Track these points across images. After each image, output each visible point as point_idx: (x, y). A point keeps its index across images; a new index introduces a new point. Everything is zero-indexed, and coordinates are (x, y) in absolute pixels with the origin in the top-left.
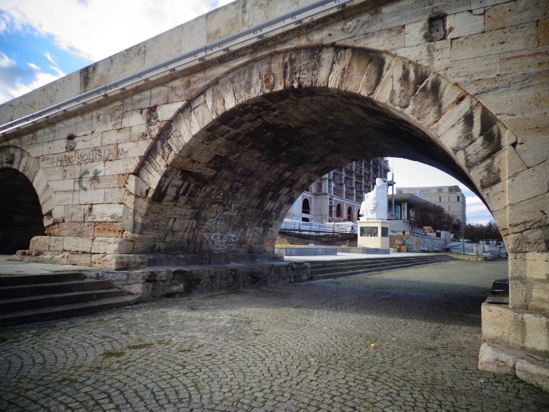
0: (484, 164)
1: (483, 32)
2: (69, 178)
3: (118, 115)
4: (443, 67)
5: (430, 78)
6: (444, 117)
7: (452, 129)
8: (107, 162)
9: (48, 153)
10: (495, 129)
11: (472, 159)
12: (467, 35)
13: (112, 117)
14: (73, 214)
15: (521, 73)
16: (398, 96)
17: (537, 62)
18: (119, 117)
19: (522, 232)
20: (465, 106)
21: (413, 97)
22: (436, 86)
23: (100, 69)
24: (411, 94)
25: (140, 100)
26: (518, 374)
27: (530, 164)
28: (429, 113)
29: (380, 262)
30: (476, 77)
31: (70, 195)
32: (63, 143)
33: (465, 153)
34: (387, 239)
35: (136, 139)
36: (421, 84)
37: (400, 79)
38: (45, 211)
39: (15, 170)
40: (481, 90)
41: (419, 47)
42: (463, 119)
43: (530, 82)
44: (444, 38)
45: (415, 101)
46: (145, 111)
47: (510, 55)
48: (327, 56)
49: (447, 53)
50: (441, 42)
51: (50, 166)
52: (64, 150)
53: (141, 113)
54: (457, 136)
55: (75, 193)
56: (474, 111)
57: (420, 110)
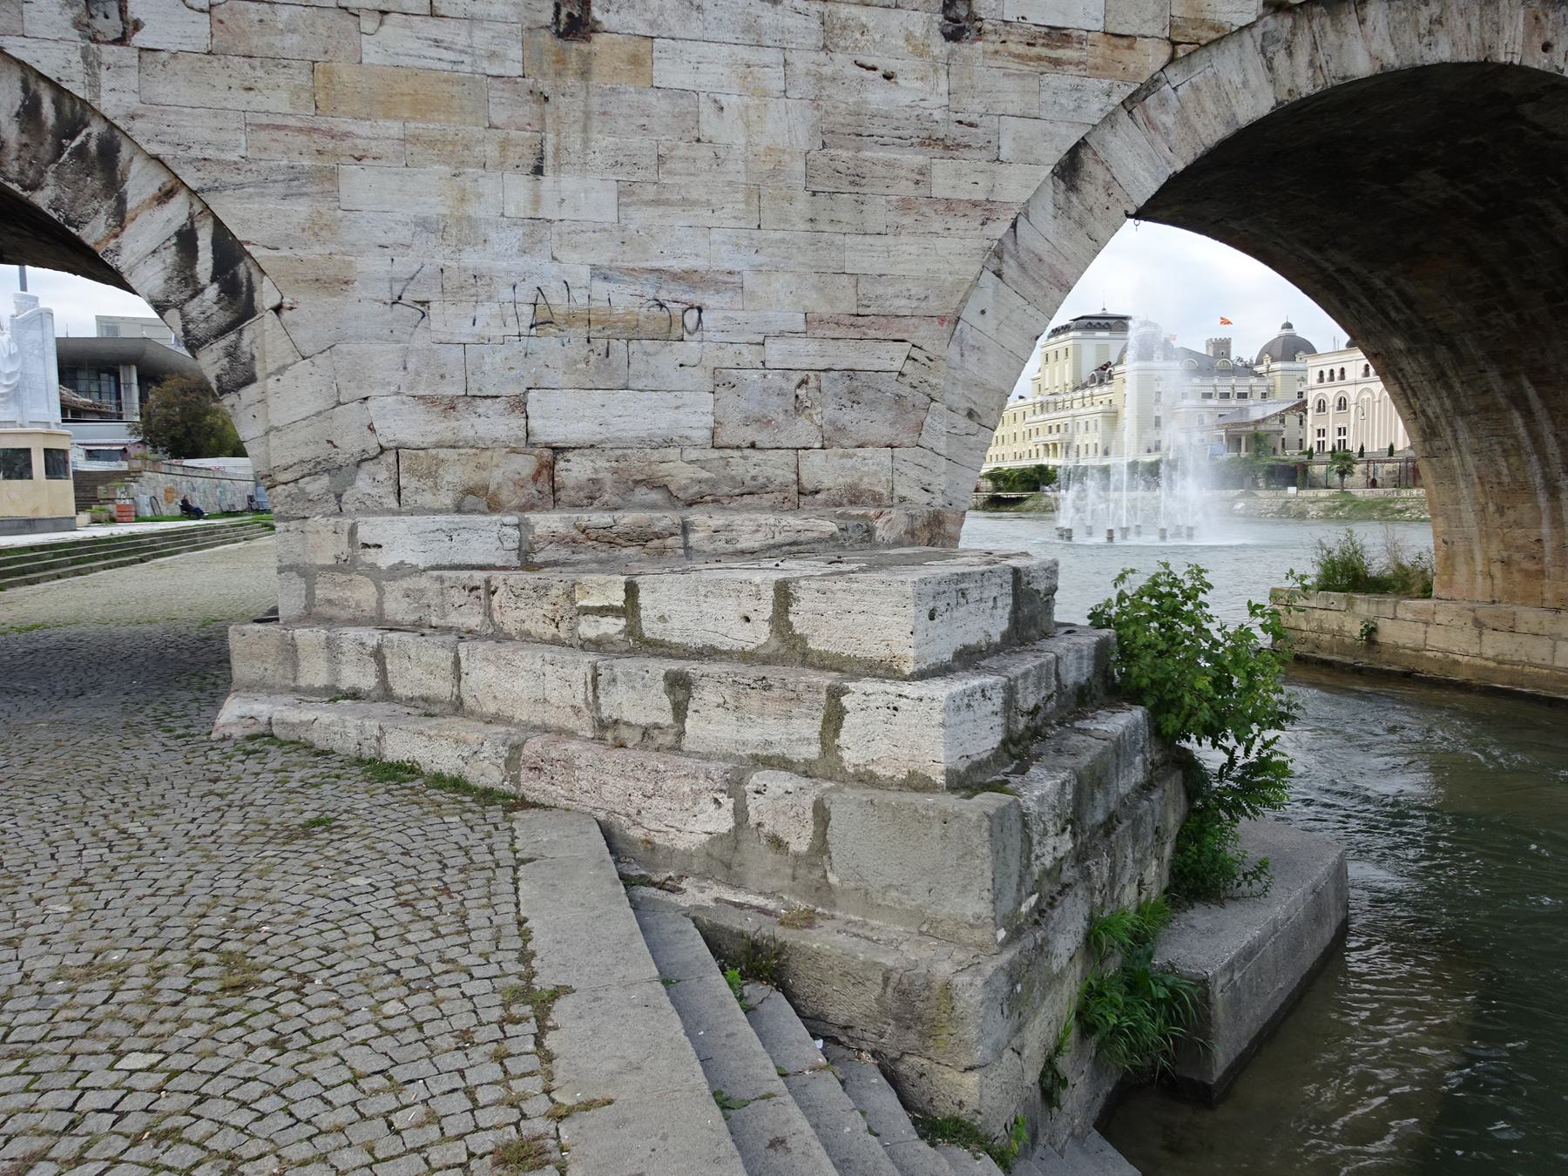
0: (223, 343)
1: (209, 53)
4: (120, 112)
5: (96, 128)
6: (131, 229)
7: (151, 260)
10: (242, 269)
11: (199, 330)
12: (174, 50)
15: (285, 162)
16: (13, 156)
17: (314, 147)
19: (296, 481)
20: (177, 211)
21: (53, 167)
22: (108, 152)
24: (47, 157)
26: (276, 730)
27: (308, 350)
28: (97, 212)
29: (37, 558)
30: (195, 152)
33: (183, 316)
34: (66, 486)
36: (73, 138)
37: (18, 115)
40: (210, 184)
41: (63, 46)
42: (174, 240)
43: (303, 185)
44: (122, 40)
45: (59, 176)
47: (264, 120)
49: (131, 79)
50: (114, 48)
54: (162, 276)
56: (197, 225)
57: (74, 200)
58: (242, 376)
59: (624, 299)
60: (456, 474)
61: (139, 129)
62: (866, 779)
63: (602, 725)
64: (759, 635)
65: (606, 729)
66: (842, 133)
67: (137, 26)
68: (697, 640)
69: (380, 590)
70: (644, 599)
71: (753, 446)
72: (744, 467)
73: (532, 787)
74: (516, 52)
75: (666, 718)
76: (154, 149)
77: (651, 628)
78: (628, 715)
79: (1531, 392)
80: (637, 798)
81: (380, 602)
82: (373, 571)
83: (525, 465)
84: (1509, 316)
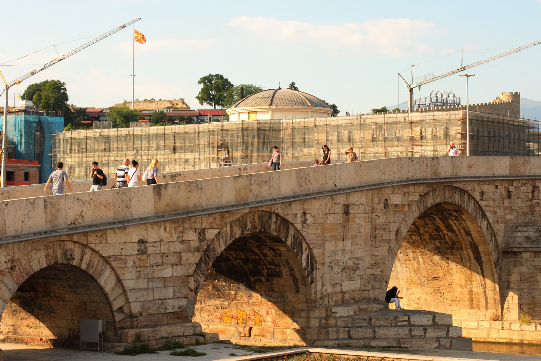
2: (143, 277)
3: (180, 230)
8: (174, 266)
9: (120, 254)
13: (176, 231)
14: (149, 308)
18: (181, 232)
23: (170, 190)
25: (195, 222)
31: (145, 293)
32: (136, 247)
35: (193, 250)
38: (115, 307)
39: (75, 267)
46: (197, 231)
48: (274, 218)
51: (123, 266)
52: (136, 252)
53: (195, 232)
55: (149, 291)
58: (312, 282)
59: (351, 263)
60: (335, 299)
61: (307, 238)
62: (452, 338)
63: (412, 336)
64: (430, 322)
65: (412, 337)
66: (375, 228)
67: (307, 220)
68: (420, 324)
69: (336, 321)
70: (411, 319)
71: (364, 290)
72: (365, 294)
73: (402, 345)
74: (342, 219)
75: (423, 334)
76: (308, 241)
77: (412, 323)
78: (416, 334)
79: (420, 257)
80: (423, 344)
81: (336, 323)
82: (336, 318)
83: (341, 296)
84: (418, 238)
